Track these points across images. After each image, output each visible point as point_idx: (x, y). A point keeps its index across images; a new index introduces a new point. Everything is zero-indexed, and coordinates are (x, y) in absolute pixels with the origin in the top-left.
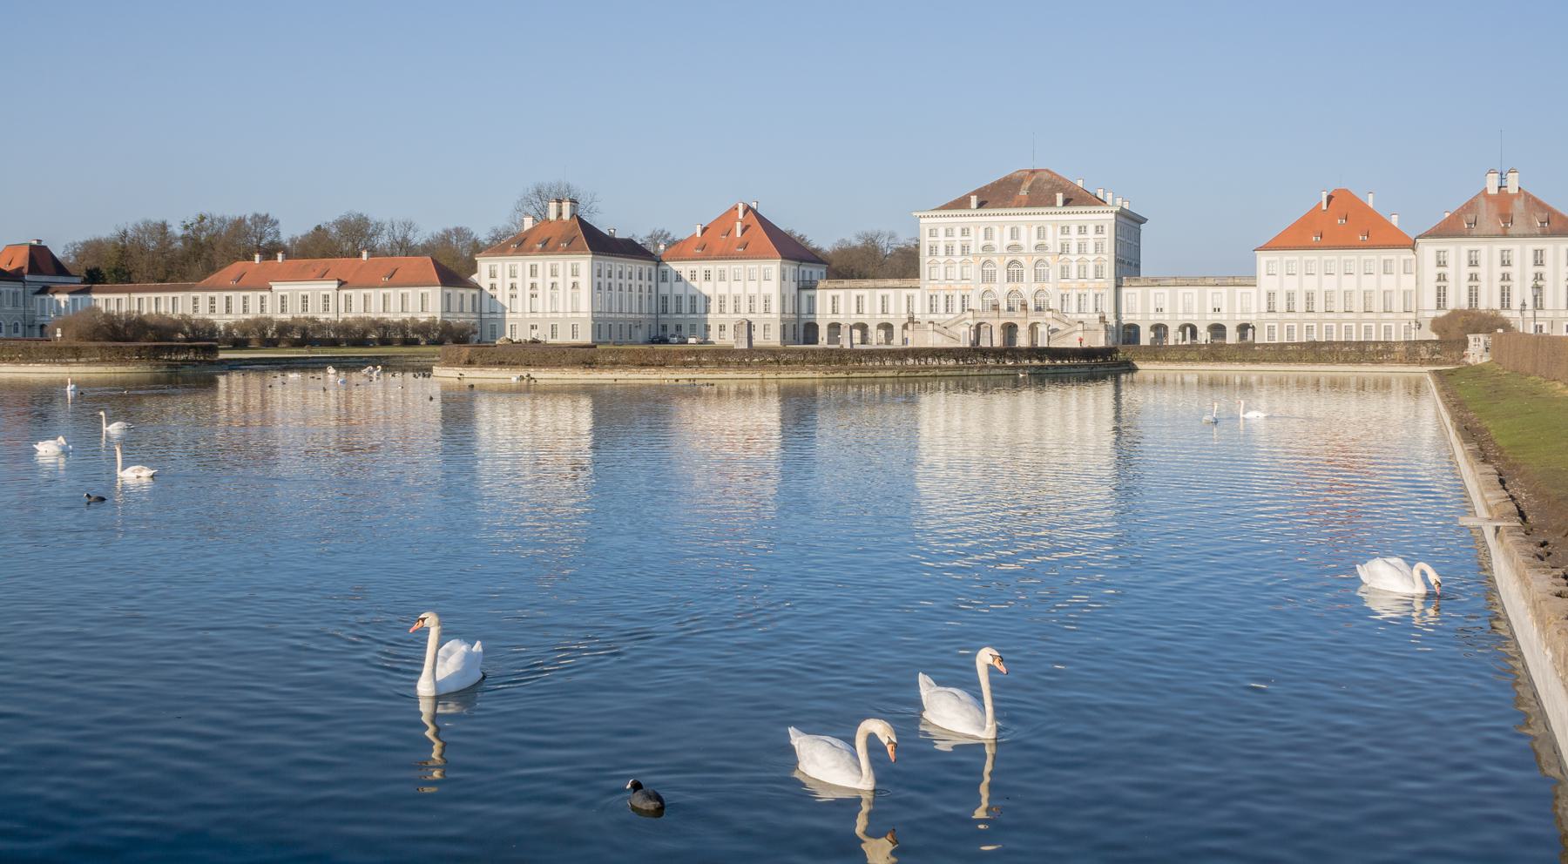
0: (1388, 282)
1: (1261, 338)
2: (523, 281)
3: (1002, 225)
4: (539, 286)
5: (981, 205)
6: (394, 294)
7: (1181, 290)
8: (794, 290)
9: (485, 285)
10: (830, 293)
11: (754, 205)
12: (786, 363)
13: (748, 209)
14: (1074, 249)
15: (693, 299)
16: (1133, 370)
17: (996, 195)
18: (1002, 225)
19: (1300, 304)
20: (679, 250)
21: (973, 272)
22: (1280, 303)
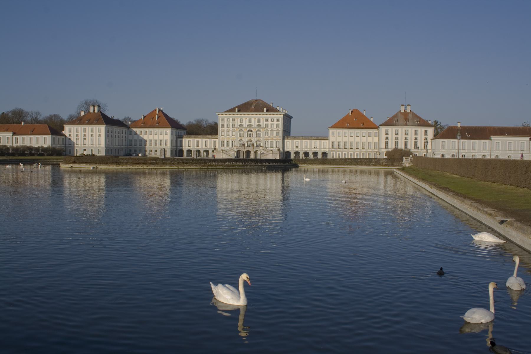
0: (370, 139)
1: (330, 157)
2: (81, 134)
3: (246, 118)
4: (87, 136)
5: (239, 111)
6: (34, 137)
7: (304, 141)
8: (175, 139)
9: (67, 135)
10: (188, 140)
11: (162, 109)
12: (186, 163)
13: (159, 110)
14: (269, 126)
15: (141, 141)
16: (298, 167)
17: (244, 108)
18: (246, 118)
19: (342, 146)
20: (136, 124)
21: (236, 133)
22: (336, 146)
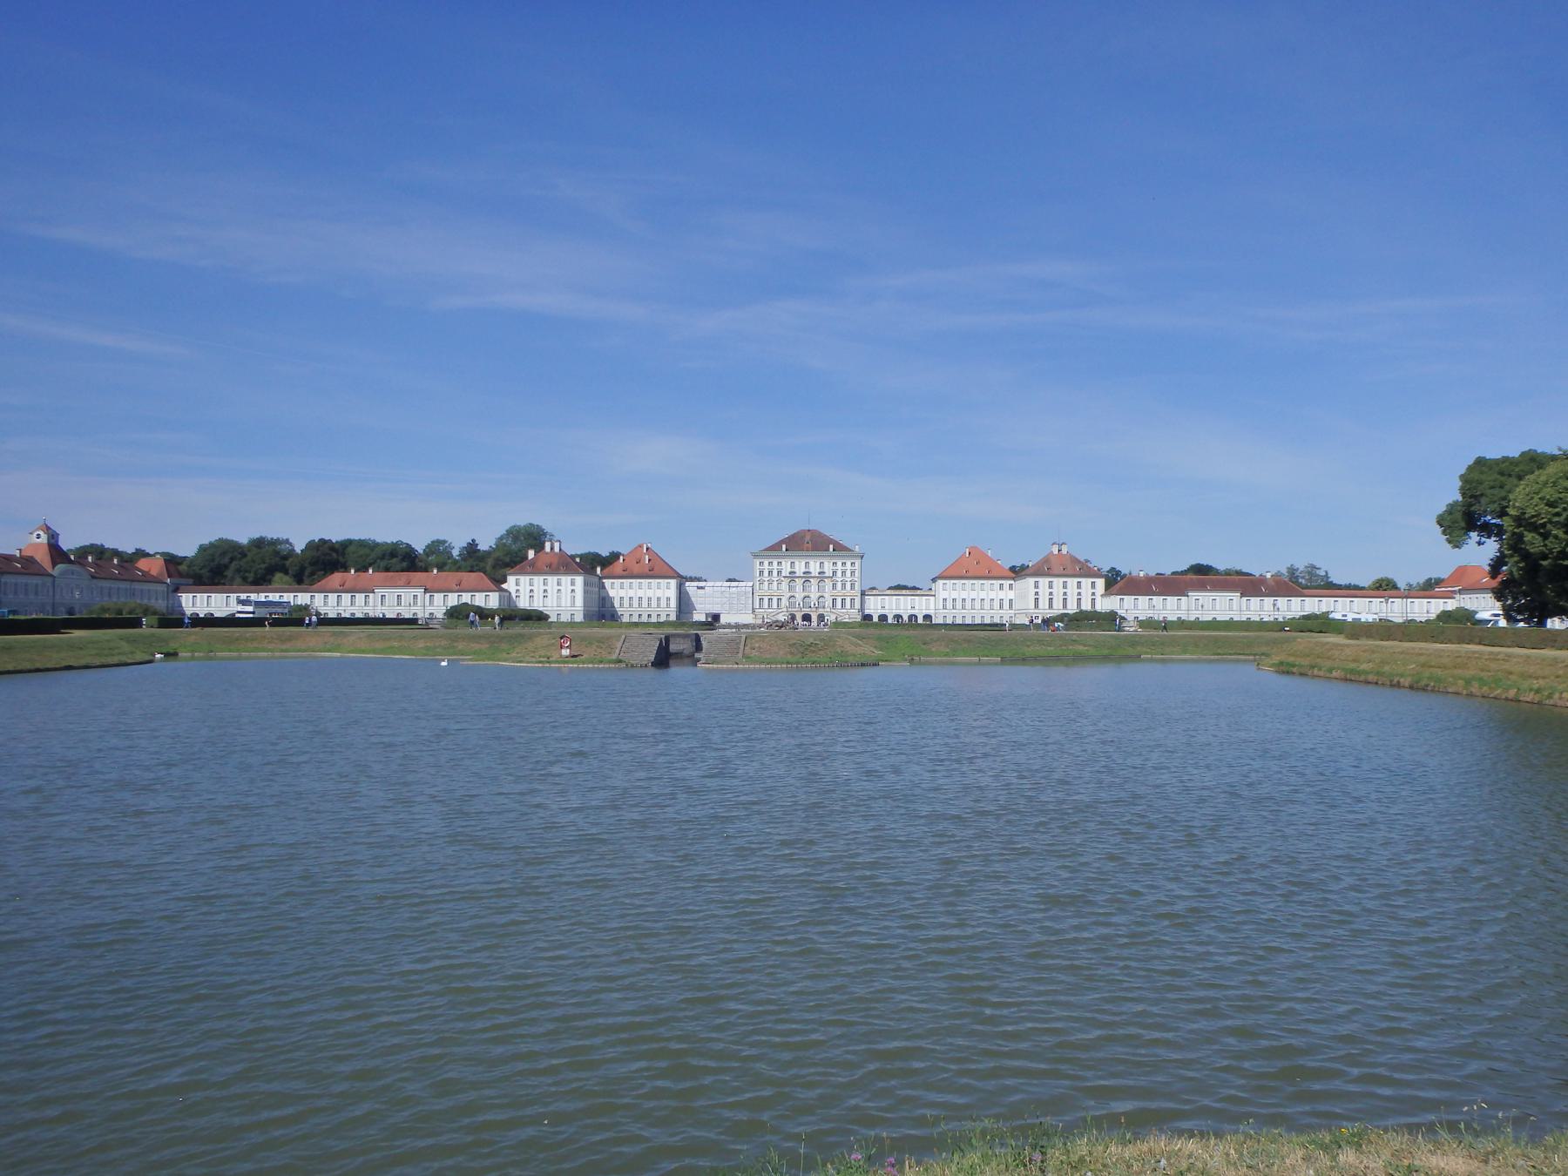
0: (1002, 595)
1: (937, 620)
14: (839, 574)
22: (949, 604)
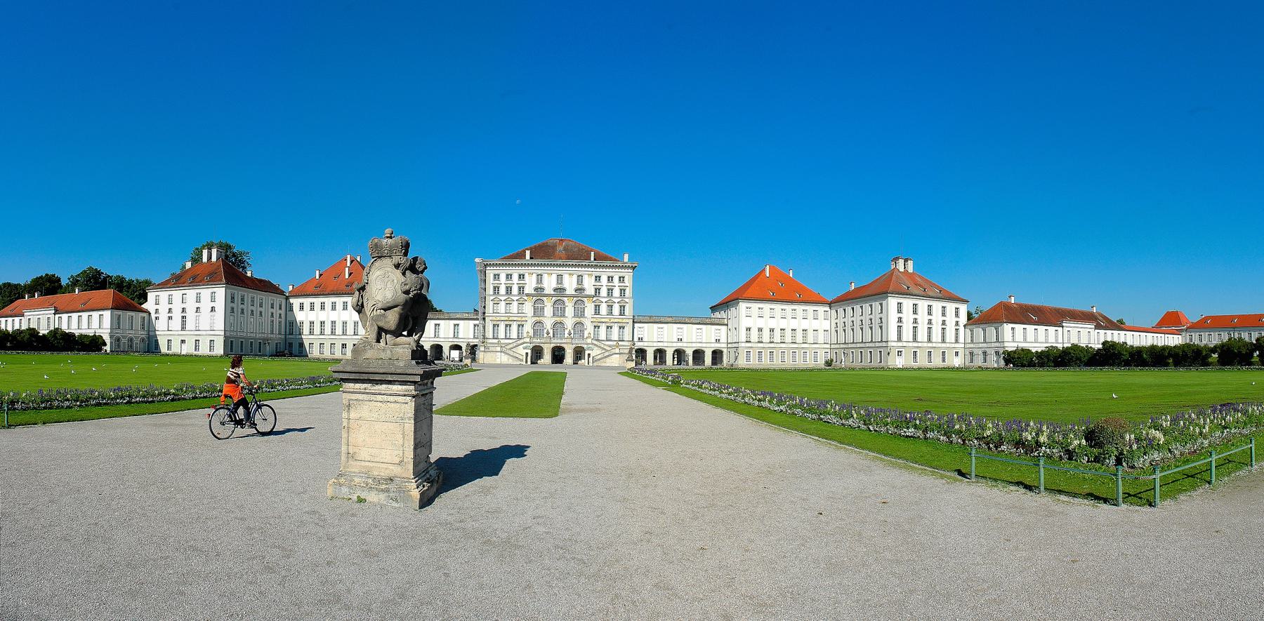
14: (604, 292)
17: (543, 253)
21: (528, 308)
